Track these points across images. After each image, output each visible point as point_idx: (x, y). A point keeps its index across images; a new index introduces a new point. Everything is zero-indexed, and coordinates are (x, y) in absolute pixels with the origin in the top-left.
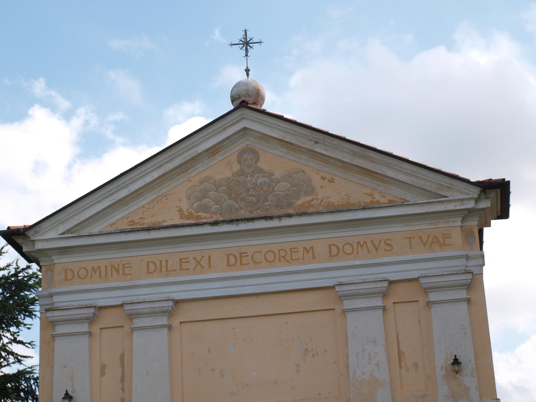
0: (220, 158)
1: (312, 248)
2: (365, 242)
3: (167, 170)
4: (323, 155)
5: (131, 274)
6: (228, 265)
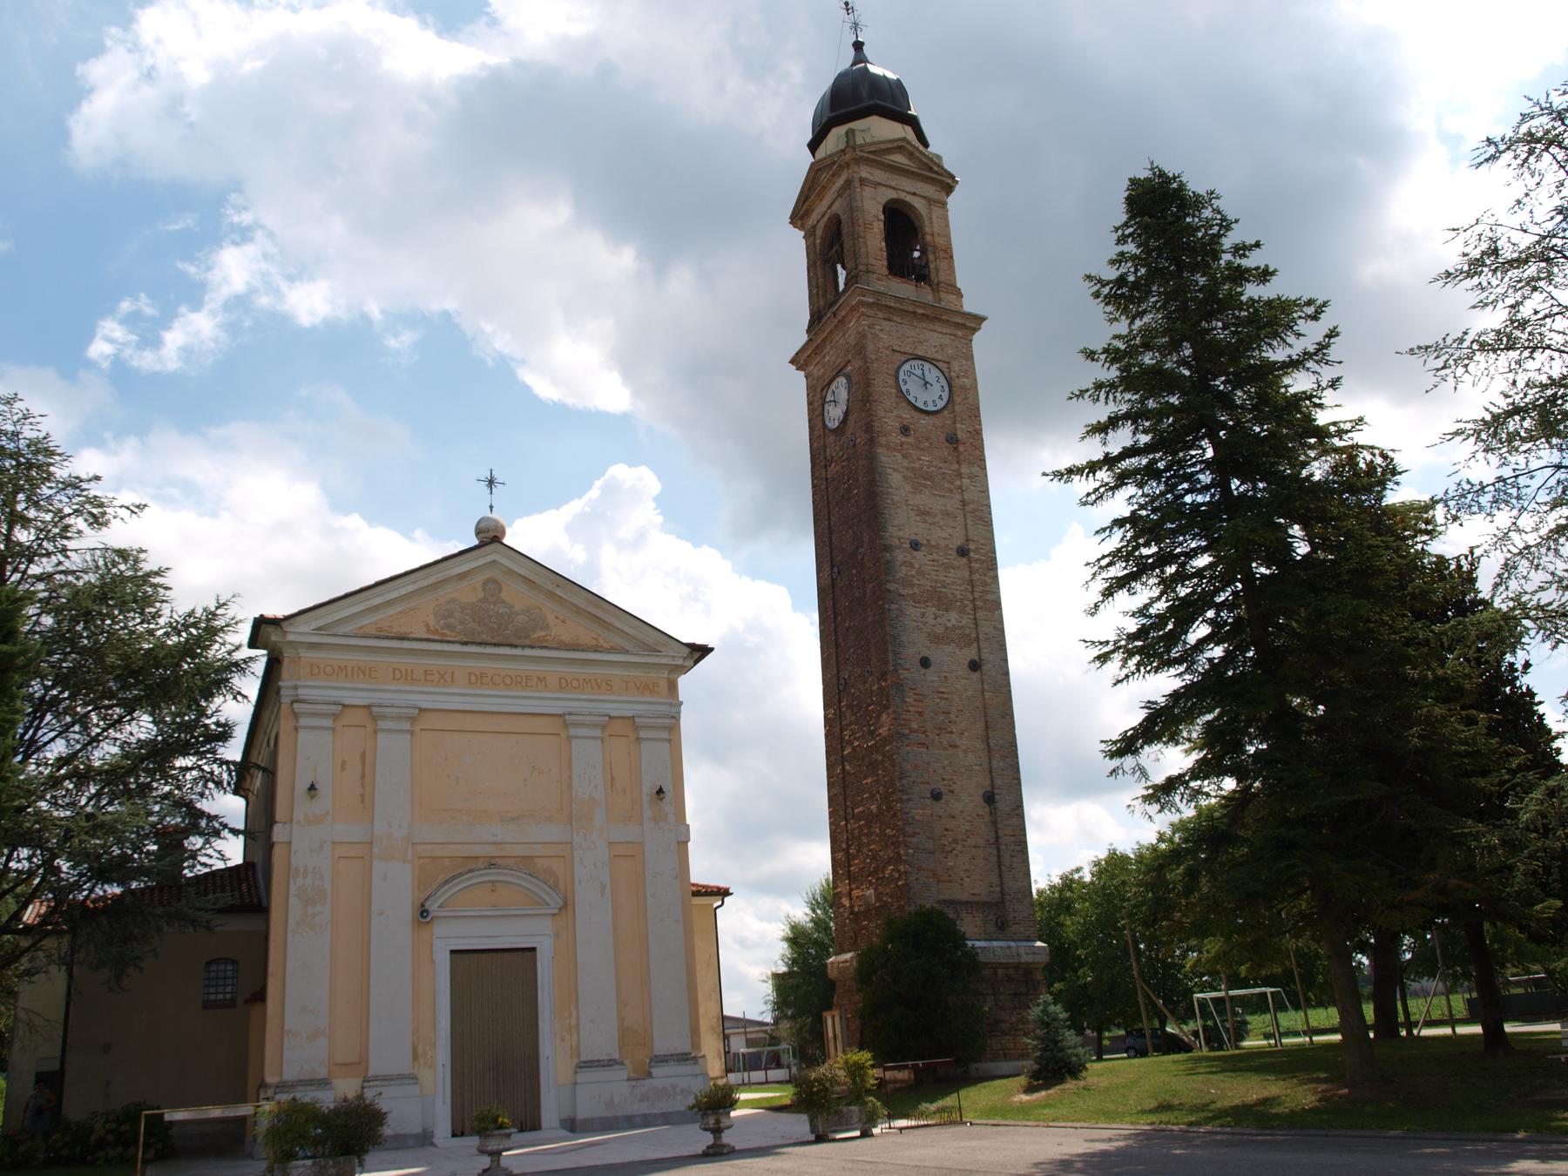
0: (466, 583)
4: (560, 597)
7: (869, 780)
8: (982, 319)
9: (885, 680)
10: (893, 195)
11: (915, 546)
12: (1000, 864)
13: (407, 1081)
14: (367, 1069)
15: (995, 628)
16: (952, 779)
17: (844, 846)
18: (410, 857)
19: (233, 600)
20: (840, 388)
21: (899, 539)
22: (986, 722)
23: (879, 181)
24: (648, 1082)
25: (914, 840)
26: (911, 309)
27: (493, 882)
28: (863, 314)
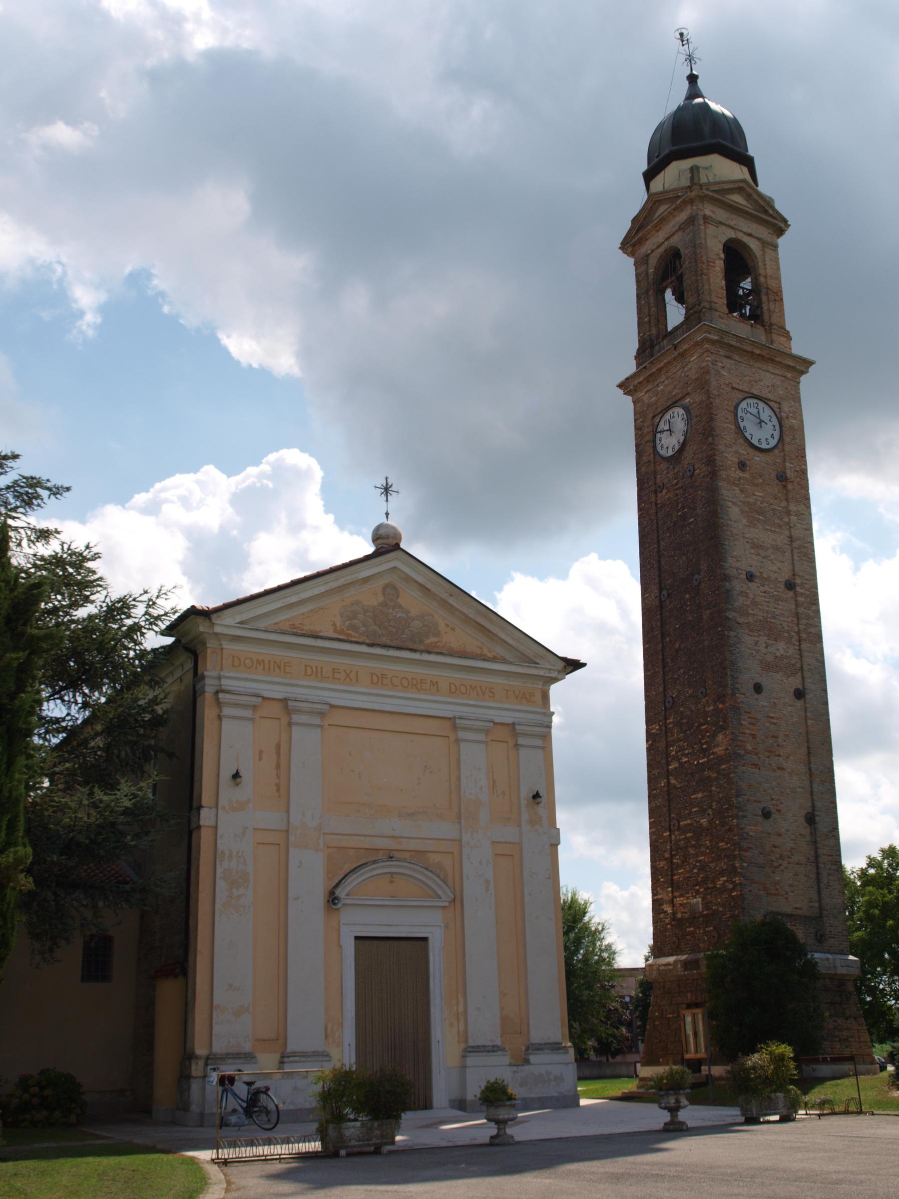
1: (437, 682)
2: (475, 687)
3: (333, 587)
4: (452, 606)
5: (291, 673)
6: (372, 682)
7: (700, 795)
8: (810, 363)
9: (723, 703)
10: (731, 234)
11: (750, 577)
12: (818, 881)
14: (285, 1045)
15: (817, 660)
16: (778, 800)
17: (667, 855)
19: (173, 590)
20: (677, 419)
21: (737, 570)
22: (808, 748)
23: (721, 220)
24: (526, 1068)
25: (748, 854)
26: (749, 348)
27: (392, 874)
28: (708, 351)
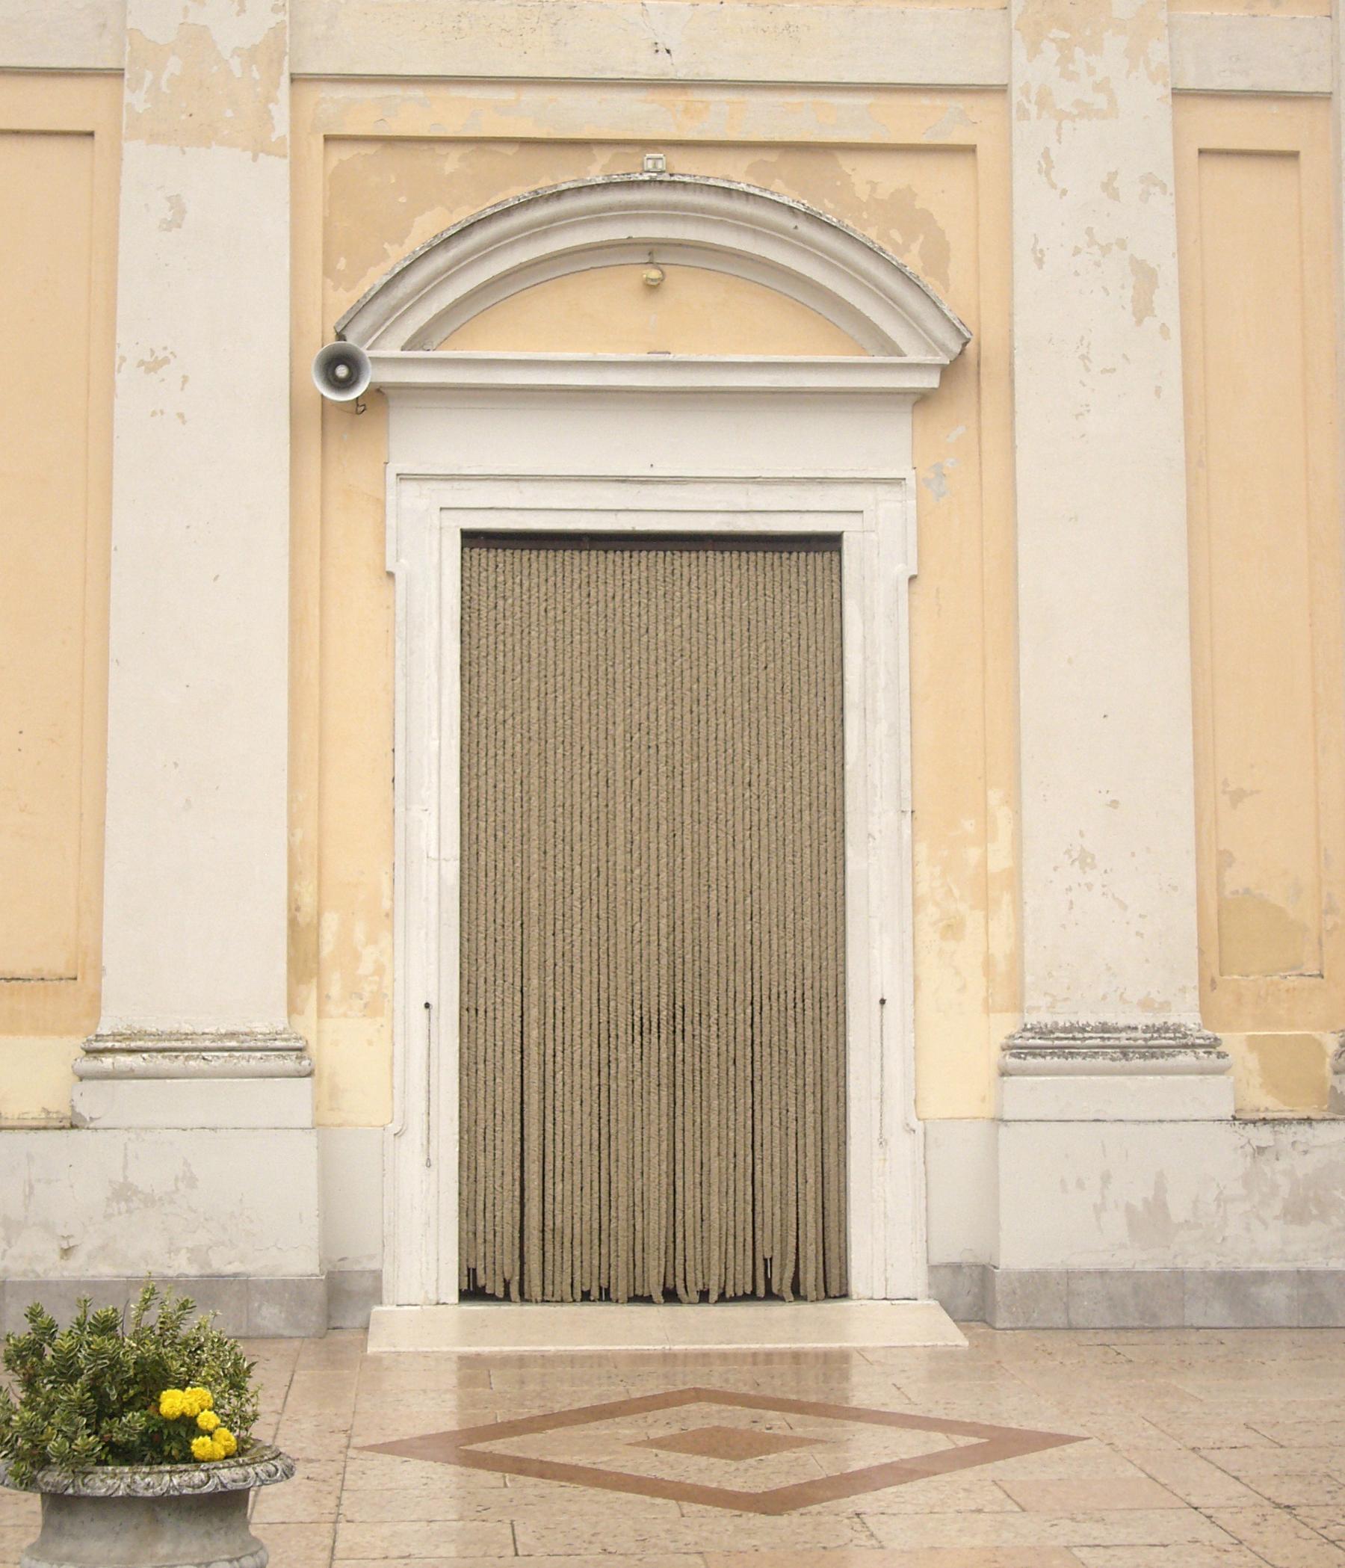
13: (254, 1062)
18: (282, 128)
